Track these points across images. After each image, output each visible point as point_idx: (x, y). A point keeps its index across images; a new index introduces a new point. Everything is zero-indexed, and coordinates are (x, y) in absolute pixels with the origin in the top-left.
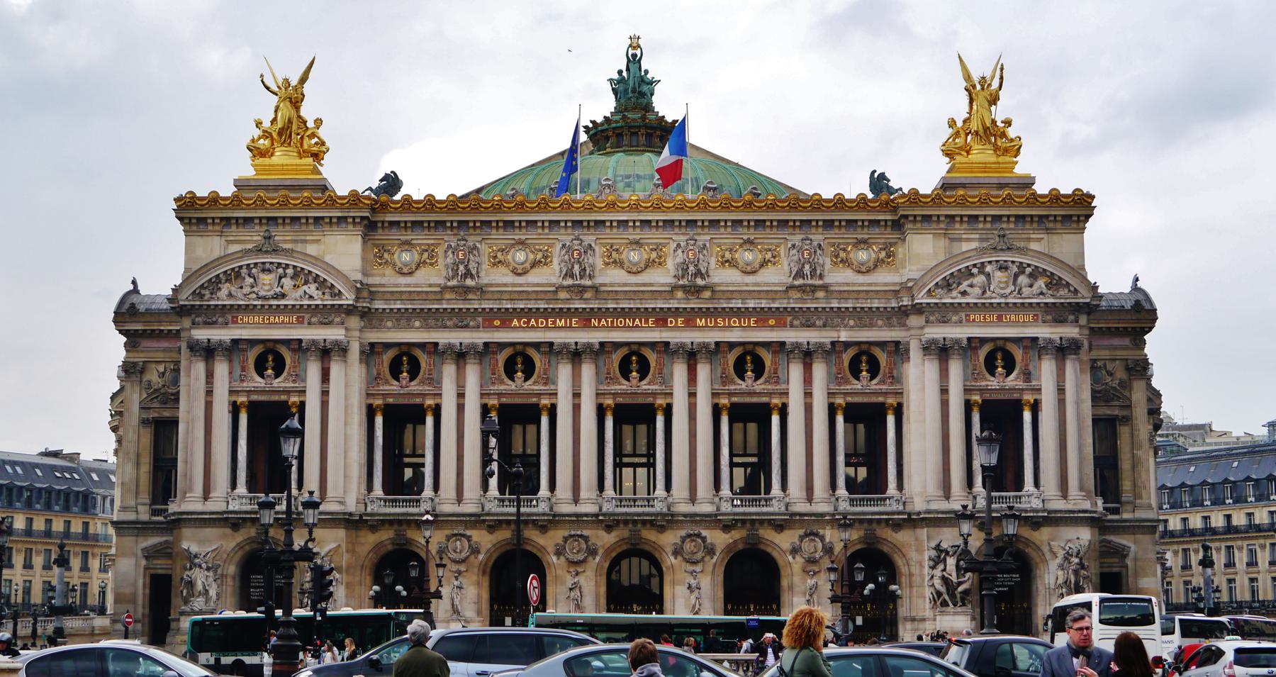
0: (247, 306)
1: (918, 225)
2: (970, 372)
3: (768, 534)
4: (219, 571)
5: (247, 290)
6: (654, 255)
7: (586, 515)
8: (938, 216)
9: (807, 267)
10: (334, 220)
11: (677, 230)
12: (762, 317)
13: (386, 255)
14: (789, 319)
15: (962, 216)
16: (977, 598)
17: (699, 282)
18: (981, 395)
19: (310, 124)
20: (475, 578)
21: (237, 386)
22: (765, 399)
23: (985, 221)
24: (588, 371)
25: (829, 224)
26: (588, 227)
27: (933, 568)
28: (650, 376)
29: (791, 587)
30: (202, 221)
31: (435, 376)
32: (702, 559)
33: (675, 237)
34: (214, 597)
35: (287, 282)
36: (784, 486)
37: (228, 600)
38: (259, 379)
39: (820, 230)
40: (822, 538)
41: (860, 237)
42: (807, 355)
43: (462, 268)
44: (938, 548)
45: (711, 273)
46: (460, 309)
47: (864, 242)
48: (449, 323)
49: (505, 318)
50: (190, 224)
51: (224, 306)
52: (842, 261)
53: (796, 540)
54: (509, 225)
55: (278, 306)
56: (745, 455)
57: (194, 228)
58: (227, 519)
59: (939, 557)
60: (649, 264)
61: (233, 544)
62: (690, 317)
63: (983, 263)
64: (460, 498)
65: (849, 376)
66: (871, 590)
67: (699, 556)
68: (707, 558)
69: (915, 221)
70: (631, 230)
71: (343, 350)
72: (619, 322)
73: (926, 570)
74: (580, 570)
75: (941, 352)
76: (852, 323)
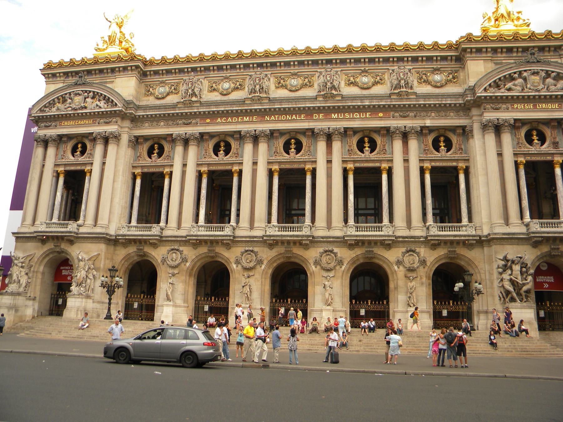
0: (66, 114)
1: (474, 55)
2: (515, 143)
3: (380, 252)
4: (32, 269)
5: (68, 105)
6: (307, 80)
7: (256, 237)
8: (487, 48)
9: (403, 82)
10: (121, 69)
11: (320, 67)
12: (374, 110)
13: (151, 90)
14: (392, 113)
15: (502, 48)
16: (533, 296)
17: (334, 92)
18: (525, 158)
19: (128, 37)
20: (183, 278)
21: (59, 162)
22: (377, 165)
23: (517, 52)
24: (263, 147)
25: (415, 59)
26: (267, 67)
27: (501, 274)
28: (302, 151)
29: (396, 288)
30: (54, 75)
31: (171, 155)
32: (335, 267)
33: (318, 70)
34: (24, 285)
35: (89, 100)
36: (391, 220)
37: (38, 288)
38: (71, 157)
39: (410, 63)
40: (418, 254)
41: (435, 67)
42: (405, 136)
43: (190, 91)
44: (505, 259)
45: (341, 90)
46: (186, 113)
47: (438, 69)
48: (180, 122)
49: (213, 115)
50: (49, 78)
51: (54, 115)
52: (424, 81)
53: (400, 255)
54: (220, 68)
55: (82, 113)
56: (366, 209)
57: (51, 80)
58: (38, 236)
59: (505, 266)
60: (304, 86)
61: (42, 252)
62: (327, 111)
63: (520, 72)
64: (179, 227)
65: (433, 149)
66: (460, 288)
67: (332, 265)
68: (338, 267)
69: (471, 52)
70: (292, 68)
71: (117, 137)
72: (283, 117)
73: (495, 275)
74: (251, 274)
75: (497, 129)
76: (433, 114)
